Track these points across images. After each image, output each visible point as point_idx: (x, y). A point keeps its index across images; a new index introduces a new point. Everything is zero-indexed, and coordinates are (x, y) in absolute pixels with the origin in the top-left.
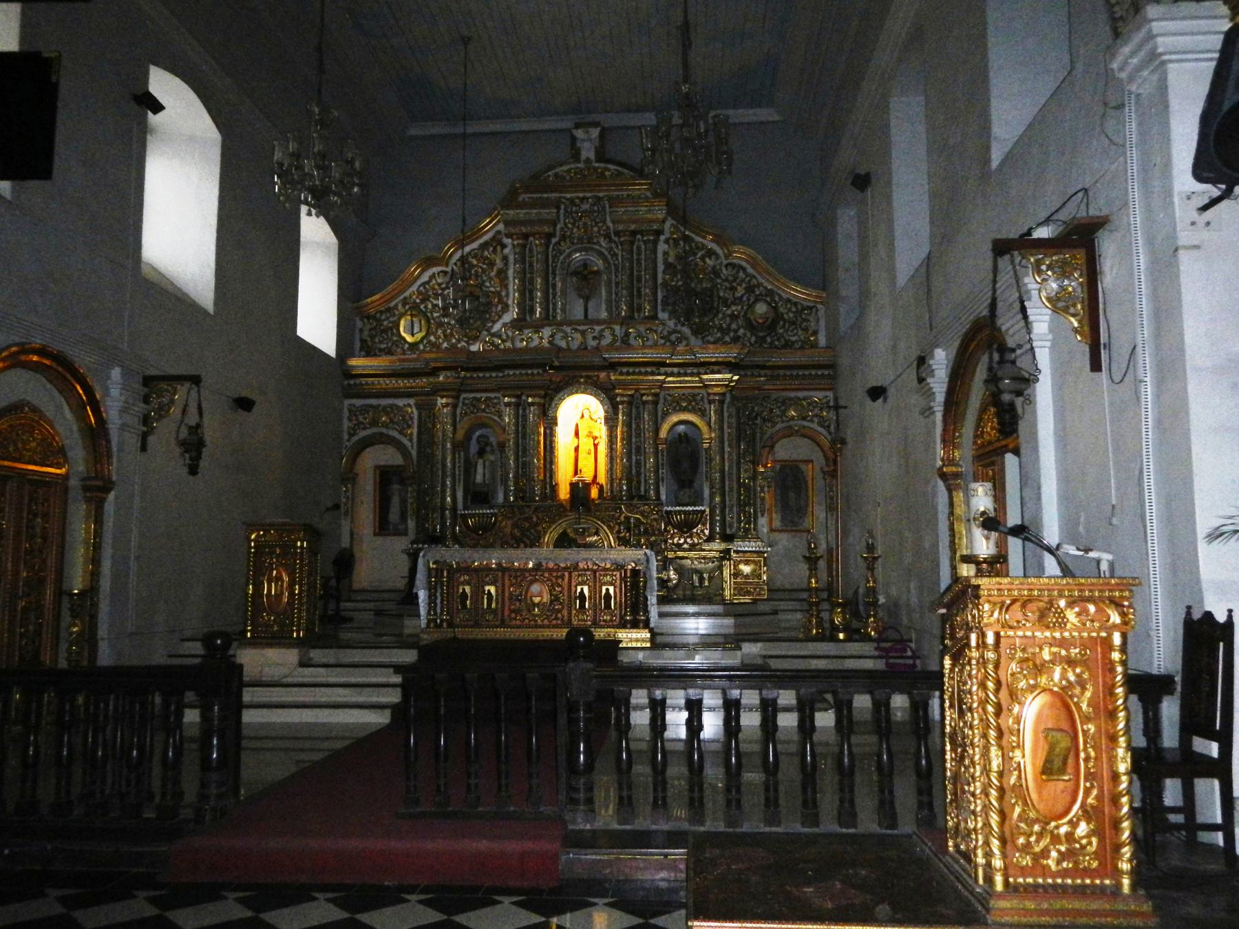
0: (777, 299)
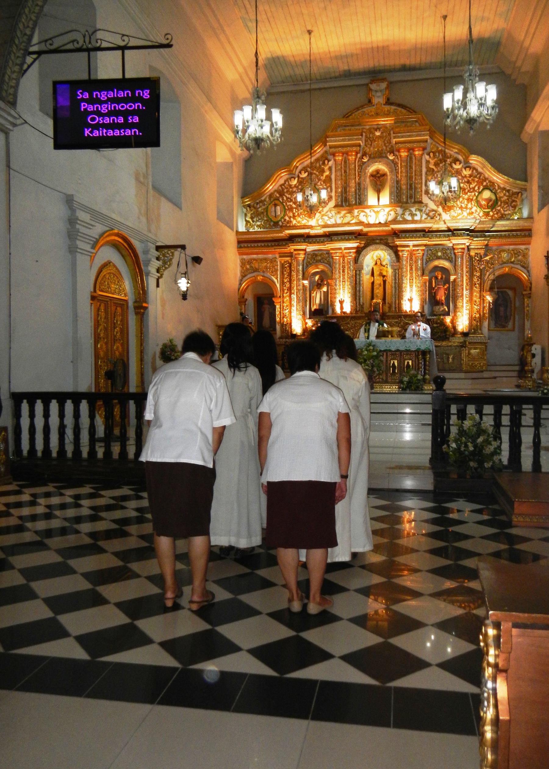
0: (497, 188)
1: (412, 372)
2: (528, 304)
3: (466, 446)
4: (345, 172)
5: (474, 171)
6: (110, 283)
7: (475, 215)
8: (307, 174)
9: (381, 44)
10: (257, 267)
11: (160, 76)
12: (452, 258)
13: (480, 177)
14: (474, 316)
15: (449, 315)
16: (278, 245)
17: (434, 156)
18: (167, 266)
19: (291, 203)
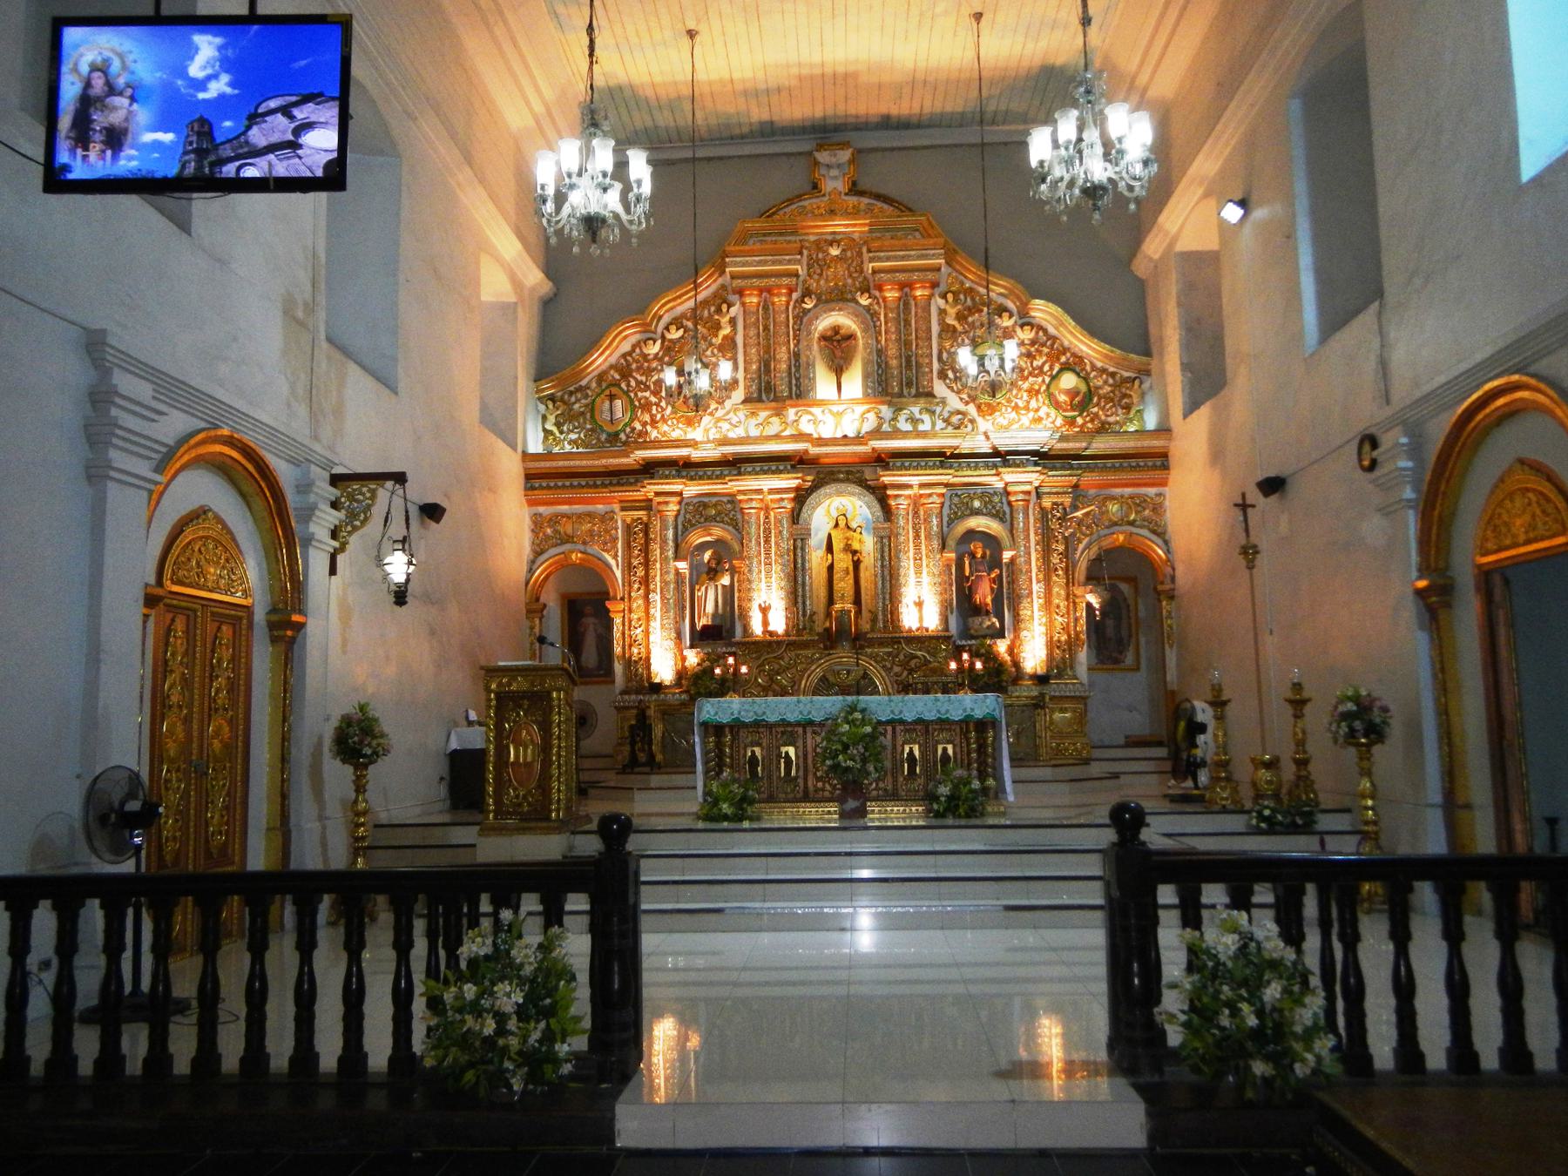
1: (959, 772)
2: (1169, 612)
3: (1235, 1012)
4: (766, 328)
5: (1041, 333)
6: (203, 562)
7: (1047, 423)
8: (681, 332)
9: (841, 69)
10: (569, 531)
11: (356, 15)
12: (1004, 513)
13: (1052, 345)
14: (1055, 638)
15: (1004, 637)
16: (619, 484)
17: (956, 300)
18: (358, 523)
19: (647, 394)
